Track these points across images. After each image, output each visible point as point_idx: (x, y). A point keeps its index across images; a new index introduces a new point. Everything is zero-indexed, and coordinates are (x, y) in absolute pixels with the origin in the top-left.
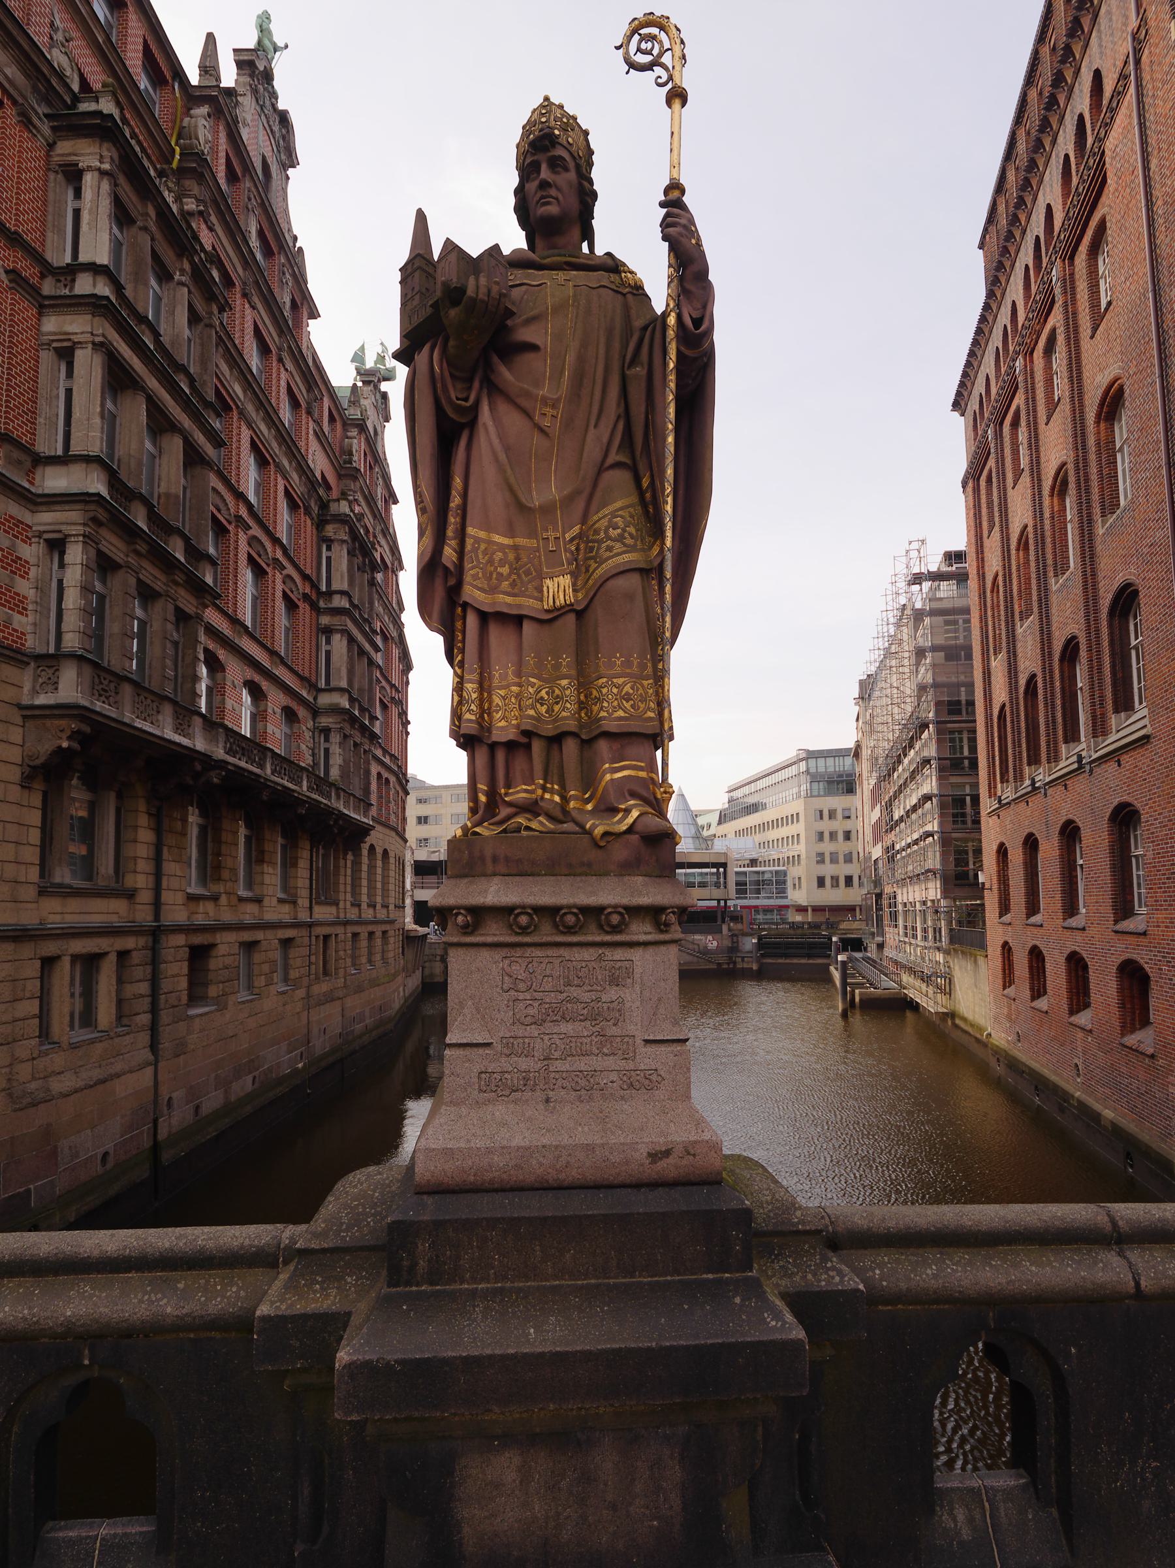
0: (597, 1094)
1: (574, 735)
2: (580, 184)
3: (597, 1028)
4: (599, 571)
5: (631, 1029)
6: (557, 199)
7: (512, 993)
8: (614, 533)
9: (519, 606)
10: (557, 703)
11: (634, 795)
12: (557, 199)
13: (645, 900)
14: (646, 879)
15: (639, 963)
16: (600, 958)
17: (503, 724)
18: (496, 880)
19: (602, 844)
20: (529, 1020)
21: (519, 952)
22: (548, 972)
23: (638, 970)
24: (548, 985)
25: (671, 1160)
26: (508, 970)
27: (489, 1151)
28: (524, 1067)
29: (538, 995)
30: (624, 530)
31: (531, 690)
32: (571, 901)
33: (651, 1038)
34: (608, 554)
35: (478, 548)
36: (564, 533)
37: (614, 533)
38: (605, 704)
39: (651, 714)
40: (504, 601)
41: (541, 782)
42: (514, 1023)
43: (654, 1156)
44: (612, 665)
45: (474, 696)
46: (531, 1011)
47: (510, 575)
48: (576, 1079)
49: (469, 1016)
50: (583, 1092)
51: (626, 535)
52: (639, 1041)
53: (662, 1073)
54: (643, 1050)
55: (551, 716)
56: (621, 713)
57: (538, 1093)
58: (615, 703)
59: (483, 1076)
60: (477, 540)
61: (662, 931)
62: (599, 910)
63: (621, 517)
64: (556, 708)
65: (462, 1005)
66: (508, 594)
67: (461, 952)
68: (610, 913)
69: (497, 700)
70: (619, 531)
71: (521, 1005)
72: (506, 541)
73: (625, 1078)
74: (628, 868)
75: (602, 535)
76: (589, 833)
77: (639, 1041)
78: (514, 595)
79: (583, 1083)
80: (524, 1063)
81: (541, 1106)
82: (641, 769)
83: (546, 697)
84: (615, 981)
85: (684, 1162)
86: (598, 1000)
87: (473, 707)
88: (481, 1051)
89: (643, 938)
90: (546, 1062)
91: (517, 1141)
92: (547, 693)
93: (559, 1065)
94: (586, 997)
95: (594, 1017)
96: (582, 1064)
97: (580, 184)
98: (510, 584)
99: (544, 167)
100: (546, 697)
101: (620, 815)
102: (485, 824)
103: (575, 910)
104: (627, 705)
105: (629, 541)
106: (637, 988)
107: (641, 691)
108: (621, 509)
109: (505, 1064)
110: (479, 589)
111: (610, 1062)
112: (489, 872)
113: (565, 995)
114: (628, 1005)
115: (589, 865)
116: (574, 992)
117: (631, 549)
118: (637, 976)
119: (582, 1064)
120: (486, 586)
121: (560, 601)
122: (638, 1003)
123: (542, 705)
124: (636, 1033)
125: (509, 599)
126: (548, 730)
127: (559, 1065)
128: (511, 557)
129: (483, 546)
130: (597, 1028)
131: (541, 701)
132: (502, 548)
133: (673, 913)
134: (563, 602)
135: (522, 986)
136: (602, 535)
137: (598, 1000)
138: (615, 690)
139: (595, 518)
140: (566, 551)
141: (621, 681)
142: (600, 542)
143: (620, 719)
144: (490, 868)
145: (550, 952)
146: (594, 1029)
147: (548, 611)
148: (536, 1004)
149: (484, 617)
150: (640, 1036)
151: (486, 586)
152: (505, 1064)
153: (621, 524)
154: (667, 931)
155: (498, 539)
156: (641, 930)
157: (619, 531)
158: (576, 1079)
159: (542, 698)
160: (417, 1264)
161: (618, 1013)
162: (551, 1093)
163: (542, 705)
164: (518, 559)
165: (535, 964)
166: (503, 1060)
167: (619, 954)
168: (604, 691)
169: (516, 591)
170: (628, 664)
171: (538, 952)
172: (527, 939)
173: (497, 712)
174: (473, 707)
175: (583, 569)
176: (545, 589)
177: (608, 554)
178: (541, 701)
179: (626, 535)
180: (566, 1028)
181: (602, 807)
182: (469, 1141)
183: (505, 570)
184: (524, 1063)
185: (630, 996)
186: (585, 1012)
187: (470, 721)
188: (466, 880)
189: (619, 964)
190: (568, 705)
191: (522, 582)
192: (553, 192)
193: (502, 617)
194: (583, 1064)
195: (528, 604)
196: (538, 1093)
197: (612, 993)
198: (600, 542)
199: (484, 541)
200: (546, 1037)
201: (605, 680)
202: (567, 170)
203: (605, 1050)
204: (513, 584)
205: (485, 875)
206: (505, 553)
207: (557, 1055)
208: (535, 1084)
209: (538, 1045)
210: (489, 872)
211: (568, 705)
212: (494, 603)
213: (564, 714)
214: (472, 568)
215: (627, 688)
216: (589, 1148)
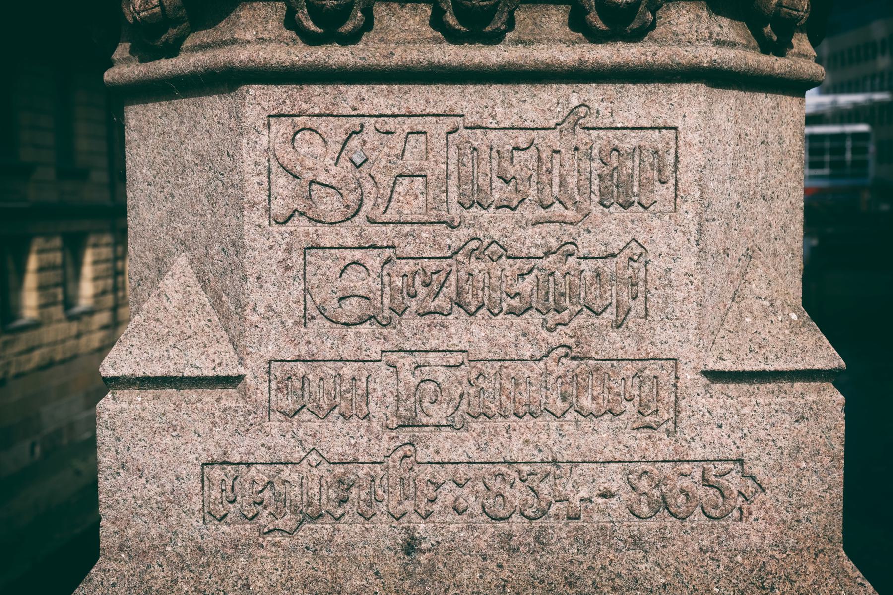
3: (561, 336)
5: (667, 338)
7: (301, 225)
15: (694, 138)
16: (575, 120)
20: (353, 307)
21: (319, 96)
22: (411, 162)
23: (692, 159)
24: (411, 201)
26: (287, 157)
28: (338, 448)
29: (378, 234)
33: (728, 365)
42: (306, 320)
46: (355, 281)
48: (497, 485)
50: (517, 523)
52: (688, 376)
53: (757, 470)
54: (704, 401)
59: (217, 473)
65: (161, 268)
71: (329, 264)
79: (517, 495)
80: (337, 437)
84: (618, 193)
86: (566, 250)
88: (209, 396)
89: (707, 54)
90: (405, 435)
93: (445, 445)
94: (531, 239)
95: (553, 303)
96: (519, 442)
106: (688, 213)
109: (278, 436)
111: (601, 437)
113: (464, 233)
114: (657, 265)
116: (494, 224)
118: (687, 177)
119: (519, 442)
122: (689, 262)
124: (685, 352)
127: (445, 445)
130: (561, 336)
137: (566, 250)
145: (417, 97)
146: (553, 339)
148: (373, 260)
150: (694, 359)
152: (278, 436)
158: (497, 485)
161: (629, 285)
162: (422, 527)
165: (370, 136)
166: (275, 424)
167: (635, 104)
171: (378, 98)
172: (338, 55)
180: (469, 334)
184: (337, 437)
185: (666, 238)
186: (526, 285)
189: (633, 140)
197: (611, 229)
200: (406, 362)
203: (587, 402)
207: (438, 413)
208: (374, 500)
209: (382, 382)
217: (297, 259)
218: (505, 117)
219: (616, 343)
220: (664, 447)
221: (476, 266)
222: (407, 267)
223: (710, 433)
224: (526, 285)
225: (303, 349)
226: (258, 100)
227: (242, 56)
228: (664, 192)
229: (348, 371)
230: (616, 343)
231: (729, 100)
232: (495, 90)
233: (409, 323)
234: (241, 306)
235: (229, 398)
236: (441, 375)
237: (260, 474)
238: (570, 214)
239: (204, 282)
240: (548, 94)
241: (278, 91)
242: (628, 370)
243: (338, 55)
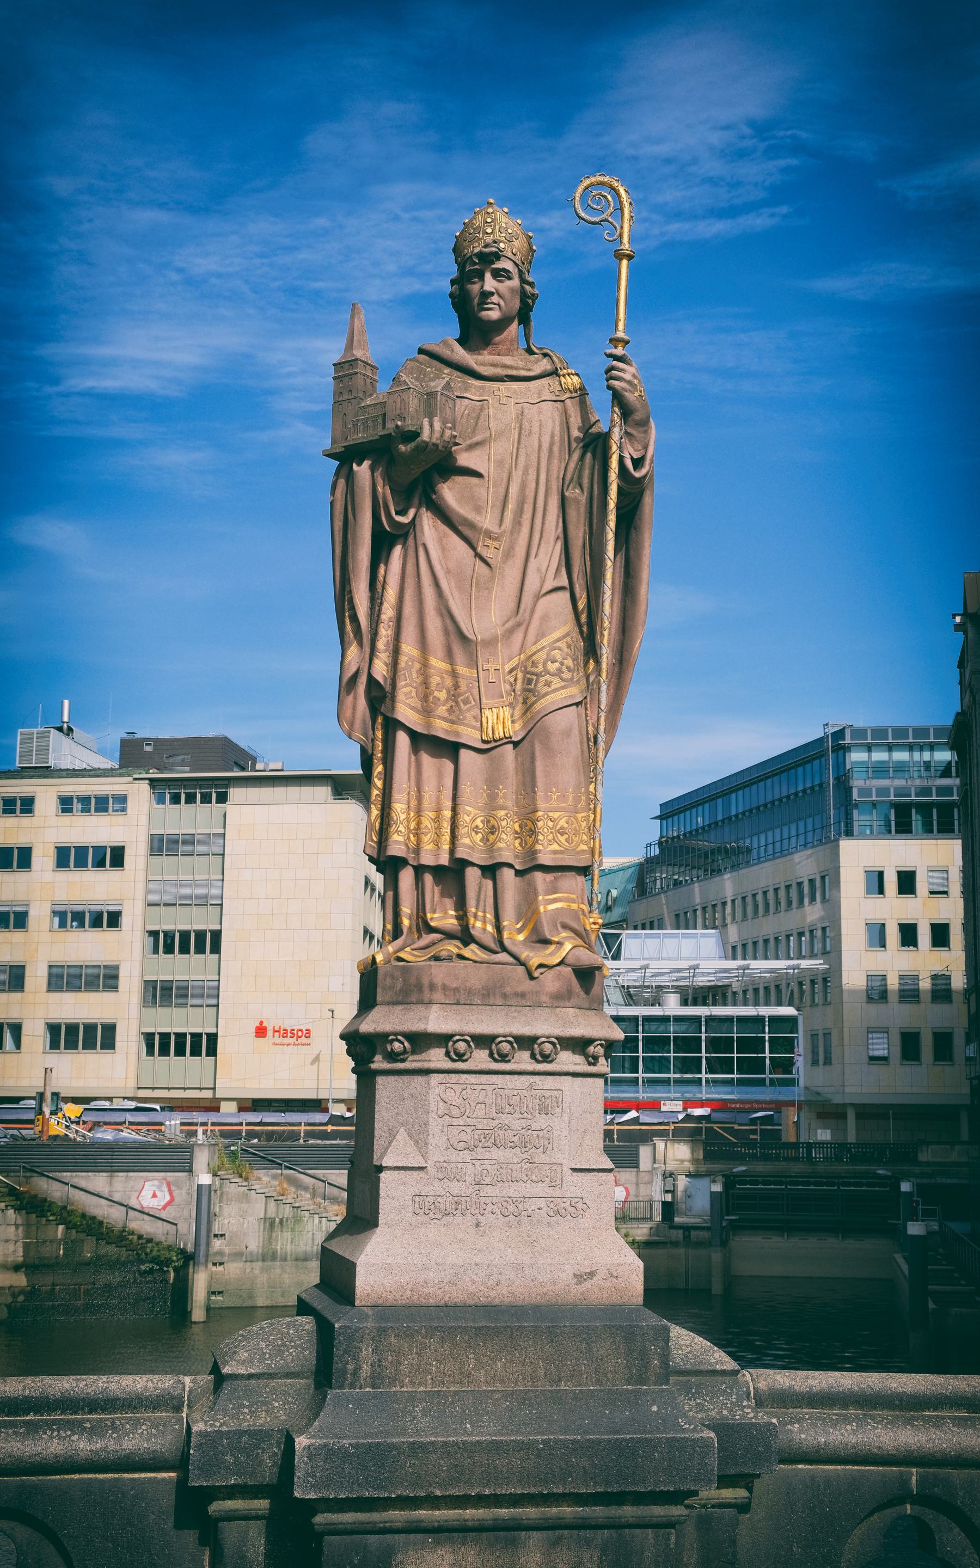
0: (525, 1220)
2: (522, 288)
3: (526, 1156)
4: (538, 706)
5: (559, 1157)
6: (498, 305)
8: (552, 667)
11: (565, 927)
12: (498, 305)
13: (577, 1031)
14: (577, 1010)
16: (531, 1087)
18: (435, 1008)
19: (536, 974)
22: (481, 1099)
23: (567, 1100)
25: (596, 1281)
27: (426, 1268)
29: (470, 1121)
30: (562, 664)
31: (466, 818)
32: (507, 1030)
33: (578, 1167)
34: (546, 689)
36: (503, 665)
37: (552, 667)
38: (541, 837)
39: (584, 847)
40: (440, 728)
41: (473, 910)
43: (580, 1278)
44: (548, 799)
45: (403, 817)
46: (463, 1137)
47: (447, 700)
48: (505, 1204)
49: (402, 1142)
51: (564, 668)
53: (587, 1202)
56: (555, 847)
57: (469, 1217)
58: (551, 837)
61: (590, 1064)
62: (533, 1039)
63: (560, 649)
64: (492, 838)
66: (445, 719)
67: (391, 1079)
68: (544, 1042)
70: (557, 665)
71: (455, 1131)
73: (552, 1205)
74: (561, 998)
75: (541, 668)
77: (566, 1170)
78: (452, 722)
79: (512, 1208)
80: (456, 1187)
81: (472, 1230)
82: (573, 901)
83: (481, 826)
85: (608, 1284)
87: (402, 828)
88: (415, 1173)
89: (572, 1068)
90: (477, 1187)
91: (452, 1259)
92: (482, 822)
93: (489, 1191)
94: (517, 1124)
95: (524, 1145)
96: (513, 1190)
97: (522, 288)
99: (488, 276)
100: (481, 826)
101: (553, 947)
102: (408, 949)
103: (511, 1039)
104: (562, 839)
105: (567, 675)
107: (575, 825)
108: (558, 640)
109: (437, 1188)
110: (413, 708)
111: (539, 1189)
112: (426, 1000)
113: (497, 1122)
115: (523, 995)
117: (569, 682)
119: (513, 1190)
121: (499, 733)
122: (566, 1133)
123: (477, 833)
124: (565, 1162)
127: (489, 1191)
128: (449, 682)
130: (526, 1156)
131: (476, 830)
133: (601, 1045)
134: (502, 735)
135: (455, 1112)
136: (541, 668)
138: (550, 824)
139: (534, 649)
140: (505, 682)
141: (555, 815)
142: (538, 675)
143: (555, 852)
144: (426, 995)
146: (524, 1156)
147: (484, 742)
148: (469, 1130)
149: (415, 736)
150: (568, 1164)
152: (437, 1188)
153: (559, 657)
154: (594, 1064)
156: (568, 1060)
157: (557, 665)
159: (477, 827)
160: (360, 1368)
162: (481, 1219)
163: (477, 833)
165: (469, 1091)
166: (436, 1183)
167: (549, 1082)
168: (540, 824)
170: (563, 798)
171: (471, 1078)
172: (460, 1066)
173: (426, 834)
174: (402, 828)
175: (521, 700)
176: (484, 719)
177: (546, 689)
178: (476, 830)
179: (564, 668)
180: (499, 1154)
182: (406, 1258)
183: (442, 695)
184: (456, 1187)
185: (558, 1124)
188: (400, 1007)
189: (549, 1093)
190: (504, 836)
191: (460, 710)
194: (512, 1191)
196: (469, 1217)
197: (541, 1122)
198: (538, 675)
202: (510, 278)
203: (534, 1178)
204: (451, 710)
205: (421, 1002)
206: (442, 678)
207: (488, 1180)
209: (470, 1170)
210: (426, 1000)
211: (504, 836)
214: (406, 686)
215: (562, 823)
216: (519, 1267)
217: (445, 1129)
218: (510, 1085)
219: (542, 1158)
220: (558, 1193)
221: (500, 1132)
222: (480, 1132)
223: (573, 1189)
224: (515, 1139)
225: (446, 1159)
226: (435, 1079)
227: (432, 1065)
228: (559, 1110)
229: (460, 1165)
230: (542, 1158)
231: (579, 1080)
232: (507, 1077)
233: (479, 1150)
234: (426, 1144)
235: (422, 1174)
236: (489, 1167)
237: (431, 1199)
238: (530, 1116)
239: (411, 1136)
240: (523, 1078)
241: (441, 1076)
242: (547, 1167)
243: (460, 1066)
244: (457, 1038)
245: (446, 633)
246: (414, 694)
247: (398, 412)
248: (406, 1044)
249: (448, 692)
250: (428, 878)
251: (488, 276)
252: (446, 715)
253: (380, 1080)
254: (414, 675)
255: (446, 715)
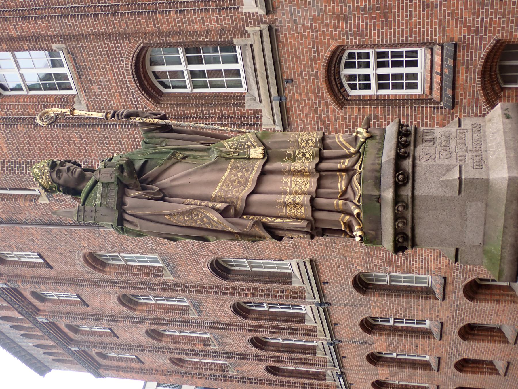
1: (320, 150)
9: (258, 167)
10: (305, 155)
17: (308, 186)
35: (224, 190)
47: (242, 172)
55: (310, 159)
60: (221, 190)
64: (308, 156)
69: (296, 188)
72: (227, 173)
76: (366, 139)
78: (253, 170)
98: (247, 172)
99: (61, 168)
110: (243, 190)
120: (243, 187)
125: (254, 172)
126: (317, 160)
128: (235, 171)
129: (224, 187)
132: (230, 174)
138: (305, 136)
151: (243, 187)
155: (224, 177)
164: (237, 168)
169: (251, 169)
173: (302, 188)
181: (354, 144)
183: (240, 174)
187: (304, 198)
192: (72, 168)
193: (259, 180)
195: (259, 164)
199: (222, 186)
201: (299, 139)
204: (247, 171)
206: (232, 174)
212: (253, 181)
213: (311, 152)
214: (232, 192)
244: (397, 180)
245: (212, 171)
246: (237, 189)
247: (109, 175)
248: (399, 221)
249: (239, 172)
250: (322, 191)
251: (61, 168)
252: (249, 173)
253: (417, 192)
254: (228, 189)
255: (249, 173)
